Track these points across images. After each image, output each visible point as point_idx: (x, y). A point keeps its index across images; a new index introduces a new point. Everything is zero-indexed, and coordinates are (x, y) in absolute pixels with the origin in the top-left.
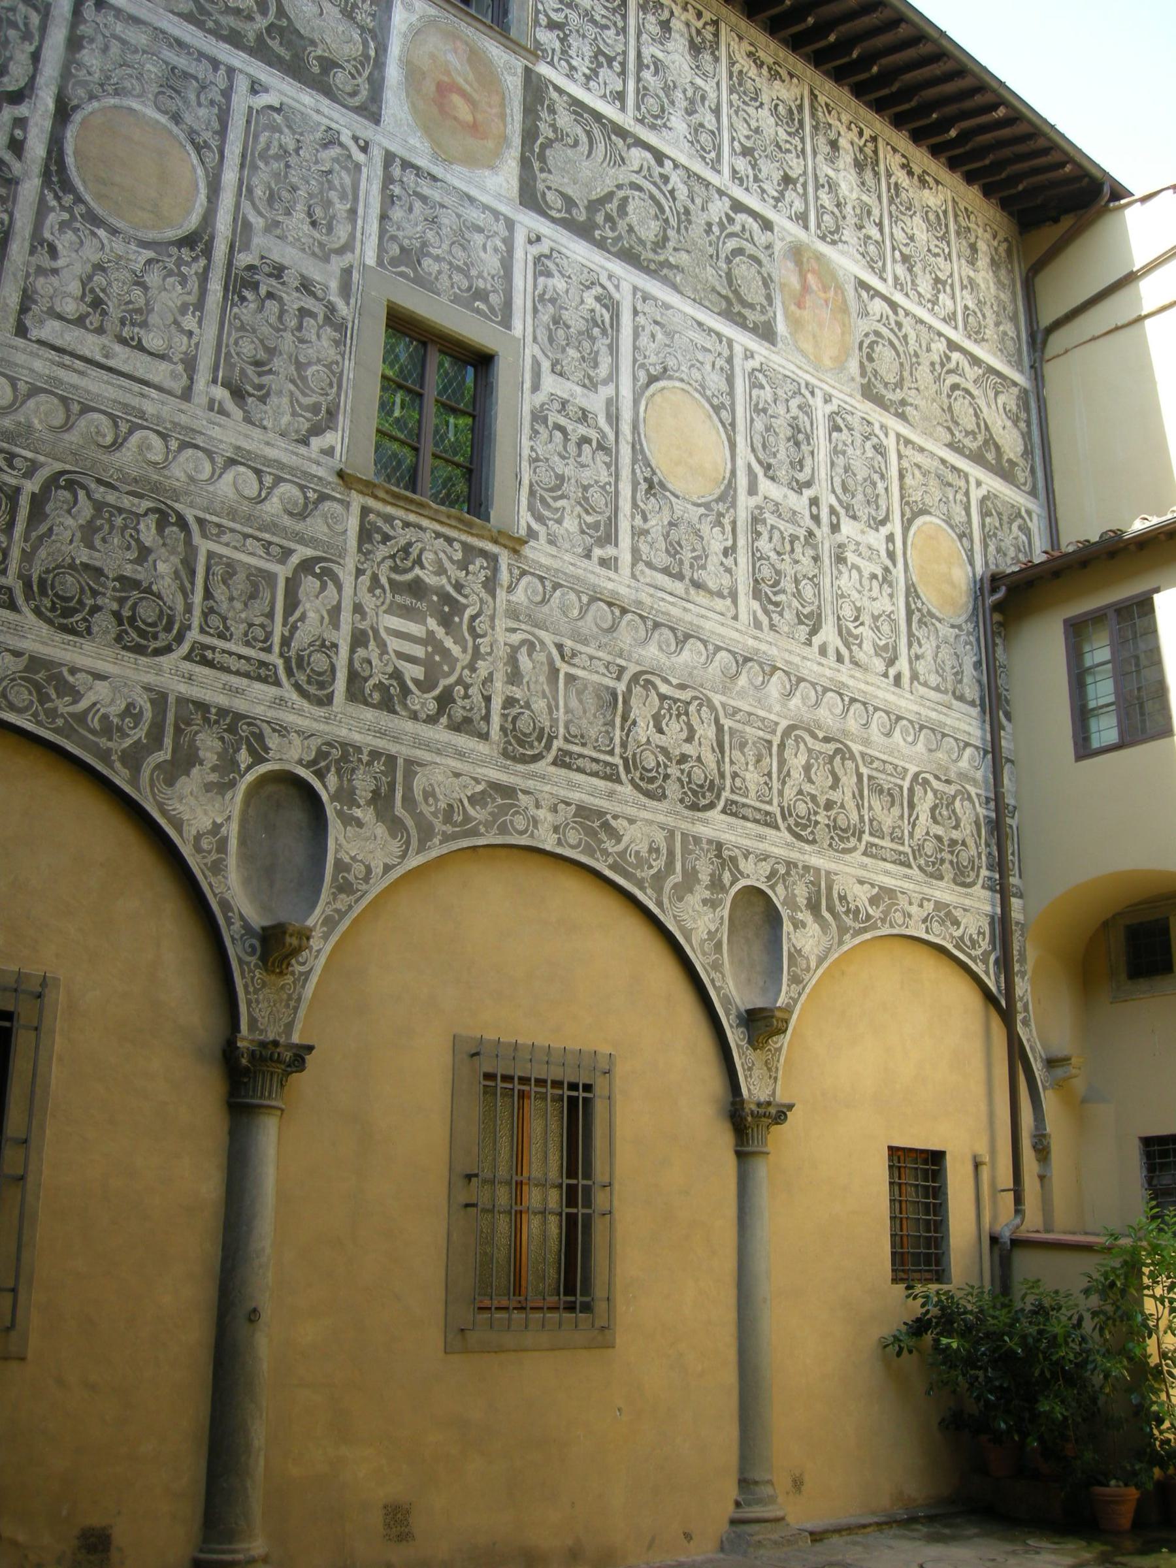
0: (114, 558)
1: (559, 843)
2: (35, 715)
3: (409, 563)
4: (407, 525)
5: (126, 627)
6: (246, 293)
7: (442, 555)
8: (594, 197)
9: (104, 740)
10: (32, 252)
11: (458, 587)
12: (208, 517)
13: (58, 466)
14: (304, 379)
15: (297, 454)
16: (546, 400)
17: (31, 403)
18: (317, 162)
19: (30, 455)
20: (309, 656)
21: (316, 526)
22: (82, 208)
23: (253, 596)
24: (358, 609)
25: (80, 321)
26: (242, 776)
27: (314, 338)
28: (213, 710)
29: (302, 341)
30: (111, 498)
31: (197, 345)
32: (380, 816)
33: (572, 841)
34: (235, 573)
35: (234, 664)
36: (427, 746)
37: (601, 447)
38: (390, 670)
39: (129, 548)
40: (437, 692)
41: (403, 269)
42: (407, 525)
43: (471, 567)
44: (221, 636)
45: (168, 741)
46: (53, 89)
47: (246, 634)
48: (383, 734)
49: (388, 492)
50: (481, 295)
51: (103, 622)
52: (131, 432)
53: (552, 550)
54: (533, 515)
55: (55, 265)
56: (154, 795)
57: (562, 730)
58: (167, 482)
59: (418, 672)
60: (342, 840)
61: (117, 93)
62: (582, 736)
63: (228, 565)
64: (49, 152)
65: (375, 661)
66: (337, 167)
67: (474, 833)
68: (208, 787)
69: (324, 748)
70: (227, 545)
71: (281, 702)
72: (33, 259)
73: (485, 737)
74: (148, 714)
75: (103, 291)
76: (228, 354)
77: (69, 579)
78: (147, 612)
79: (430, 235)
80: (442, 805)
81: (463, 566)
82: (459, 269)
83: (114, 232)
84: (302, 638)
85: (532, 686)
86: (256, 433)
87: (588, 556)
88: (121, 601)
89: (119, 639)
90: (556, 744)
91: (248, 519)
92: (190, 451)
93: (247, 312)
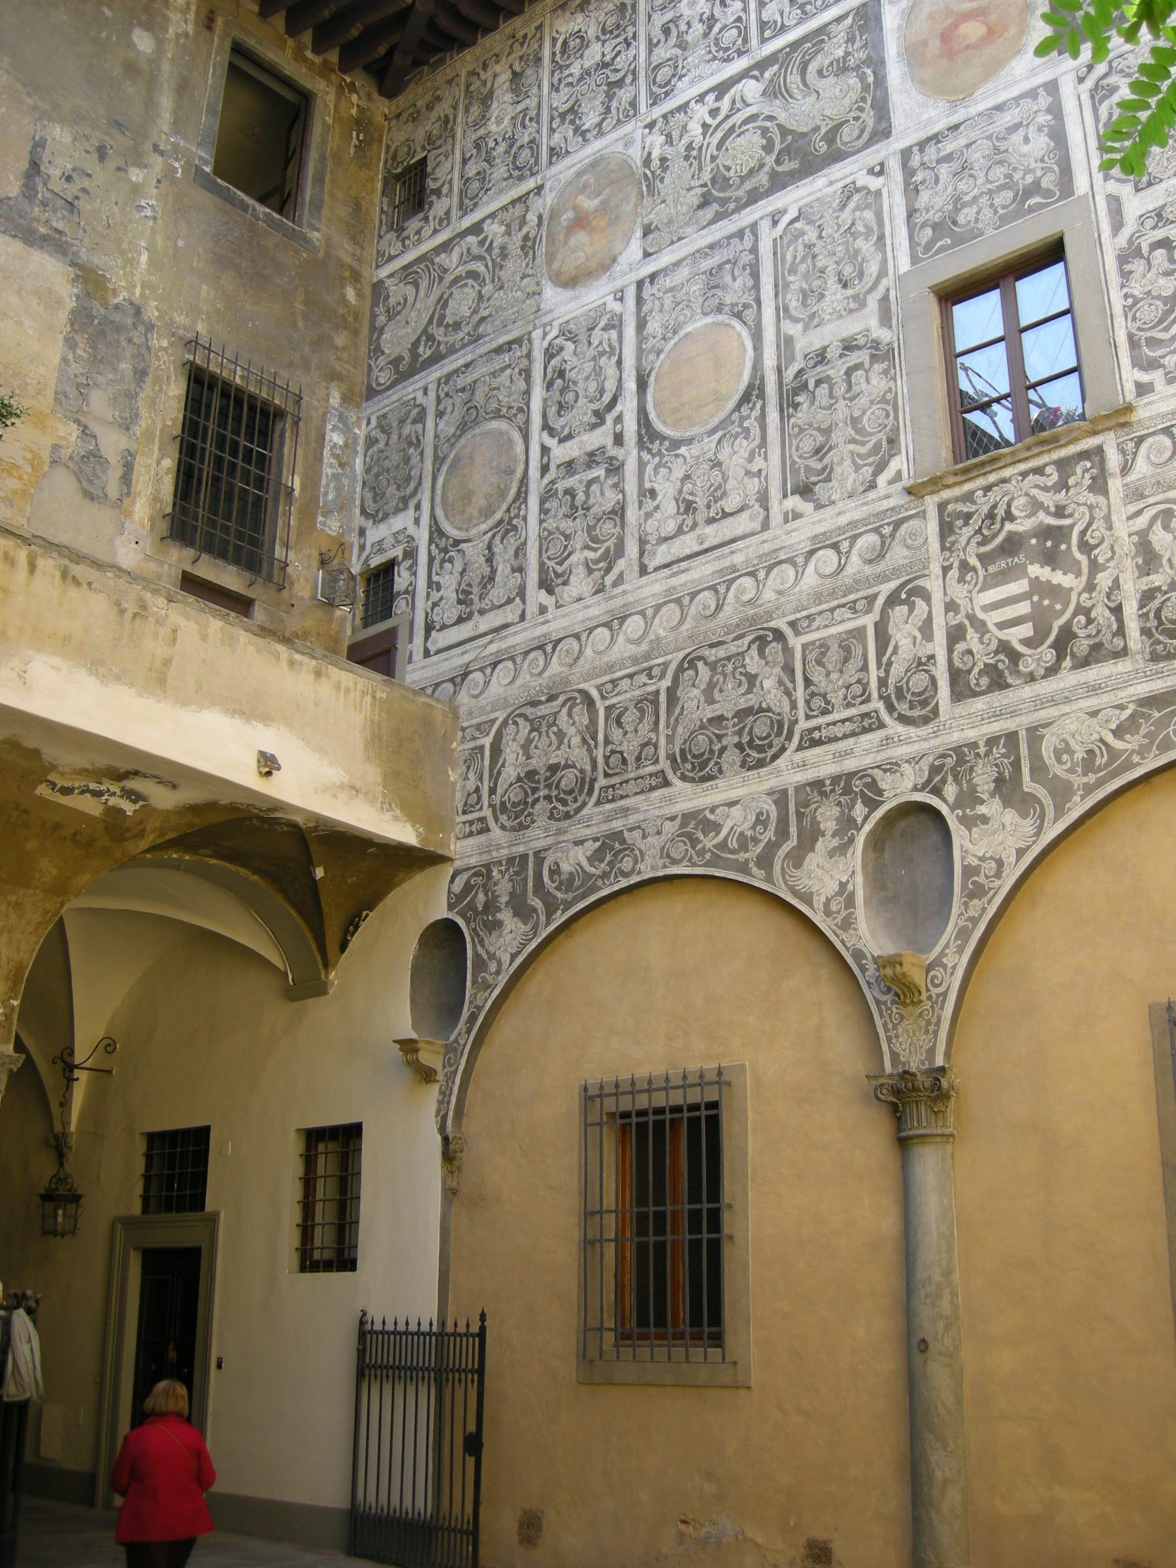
2: (690, 861)
3: (998, 526)
4: (987, 489)
5: (748, 751)
6: (799, 399)
7: (1035, 492)
10: (641, 503)
11: (1060, 512)
12: (798, 616)
13: (681, 655)
14: (859, 431)
15: (866, 504)
17: (657, 621)
18: (839, 226)
19: (660, 660)
21: (898, 555)
22: (667, 443)
23: (846, 660)
24: (951, 607)
25: (680, 531)
26: (859, 830)
27: (864, 385)
28: (828, 782)
30: (721, 653)
31: (766, 478)
32: (1007, 803)
34: (828, 649)
35: (839, 731)
36: (1053, 701)
38: (994, 645)
39: (740, 685)
42: (987, 489)
43: (1071, 481)
44: (825, 712)
45: (793, 830)
46: (634, 373)
47: (845, 698)
48: (998, 715)
49: (955, 474)
50: (1035, 188)
51: (732, 757)
52: (728, 589)
55: (656, 503)
58: (760, 610)
59: (1026, 630)
60: (967, 844)
61: (675, 332)
63: (821, 646)
65: (975, 646)
66: (858, 213)
67: (1128, 766)
68: (831, 854)
71: (888, 741)
73: (1124, 652)
74: (774, 815)
75: (692, 494)
77: (700, 737)
79: (962, 186)
80: (1080, 755)
81: (1063, 485)
82: (1000, 188)
84: (897, 670)
86: (828, 512)
88: (739, 733)
89: (743, 764)
91: (833, 594)
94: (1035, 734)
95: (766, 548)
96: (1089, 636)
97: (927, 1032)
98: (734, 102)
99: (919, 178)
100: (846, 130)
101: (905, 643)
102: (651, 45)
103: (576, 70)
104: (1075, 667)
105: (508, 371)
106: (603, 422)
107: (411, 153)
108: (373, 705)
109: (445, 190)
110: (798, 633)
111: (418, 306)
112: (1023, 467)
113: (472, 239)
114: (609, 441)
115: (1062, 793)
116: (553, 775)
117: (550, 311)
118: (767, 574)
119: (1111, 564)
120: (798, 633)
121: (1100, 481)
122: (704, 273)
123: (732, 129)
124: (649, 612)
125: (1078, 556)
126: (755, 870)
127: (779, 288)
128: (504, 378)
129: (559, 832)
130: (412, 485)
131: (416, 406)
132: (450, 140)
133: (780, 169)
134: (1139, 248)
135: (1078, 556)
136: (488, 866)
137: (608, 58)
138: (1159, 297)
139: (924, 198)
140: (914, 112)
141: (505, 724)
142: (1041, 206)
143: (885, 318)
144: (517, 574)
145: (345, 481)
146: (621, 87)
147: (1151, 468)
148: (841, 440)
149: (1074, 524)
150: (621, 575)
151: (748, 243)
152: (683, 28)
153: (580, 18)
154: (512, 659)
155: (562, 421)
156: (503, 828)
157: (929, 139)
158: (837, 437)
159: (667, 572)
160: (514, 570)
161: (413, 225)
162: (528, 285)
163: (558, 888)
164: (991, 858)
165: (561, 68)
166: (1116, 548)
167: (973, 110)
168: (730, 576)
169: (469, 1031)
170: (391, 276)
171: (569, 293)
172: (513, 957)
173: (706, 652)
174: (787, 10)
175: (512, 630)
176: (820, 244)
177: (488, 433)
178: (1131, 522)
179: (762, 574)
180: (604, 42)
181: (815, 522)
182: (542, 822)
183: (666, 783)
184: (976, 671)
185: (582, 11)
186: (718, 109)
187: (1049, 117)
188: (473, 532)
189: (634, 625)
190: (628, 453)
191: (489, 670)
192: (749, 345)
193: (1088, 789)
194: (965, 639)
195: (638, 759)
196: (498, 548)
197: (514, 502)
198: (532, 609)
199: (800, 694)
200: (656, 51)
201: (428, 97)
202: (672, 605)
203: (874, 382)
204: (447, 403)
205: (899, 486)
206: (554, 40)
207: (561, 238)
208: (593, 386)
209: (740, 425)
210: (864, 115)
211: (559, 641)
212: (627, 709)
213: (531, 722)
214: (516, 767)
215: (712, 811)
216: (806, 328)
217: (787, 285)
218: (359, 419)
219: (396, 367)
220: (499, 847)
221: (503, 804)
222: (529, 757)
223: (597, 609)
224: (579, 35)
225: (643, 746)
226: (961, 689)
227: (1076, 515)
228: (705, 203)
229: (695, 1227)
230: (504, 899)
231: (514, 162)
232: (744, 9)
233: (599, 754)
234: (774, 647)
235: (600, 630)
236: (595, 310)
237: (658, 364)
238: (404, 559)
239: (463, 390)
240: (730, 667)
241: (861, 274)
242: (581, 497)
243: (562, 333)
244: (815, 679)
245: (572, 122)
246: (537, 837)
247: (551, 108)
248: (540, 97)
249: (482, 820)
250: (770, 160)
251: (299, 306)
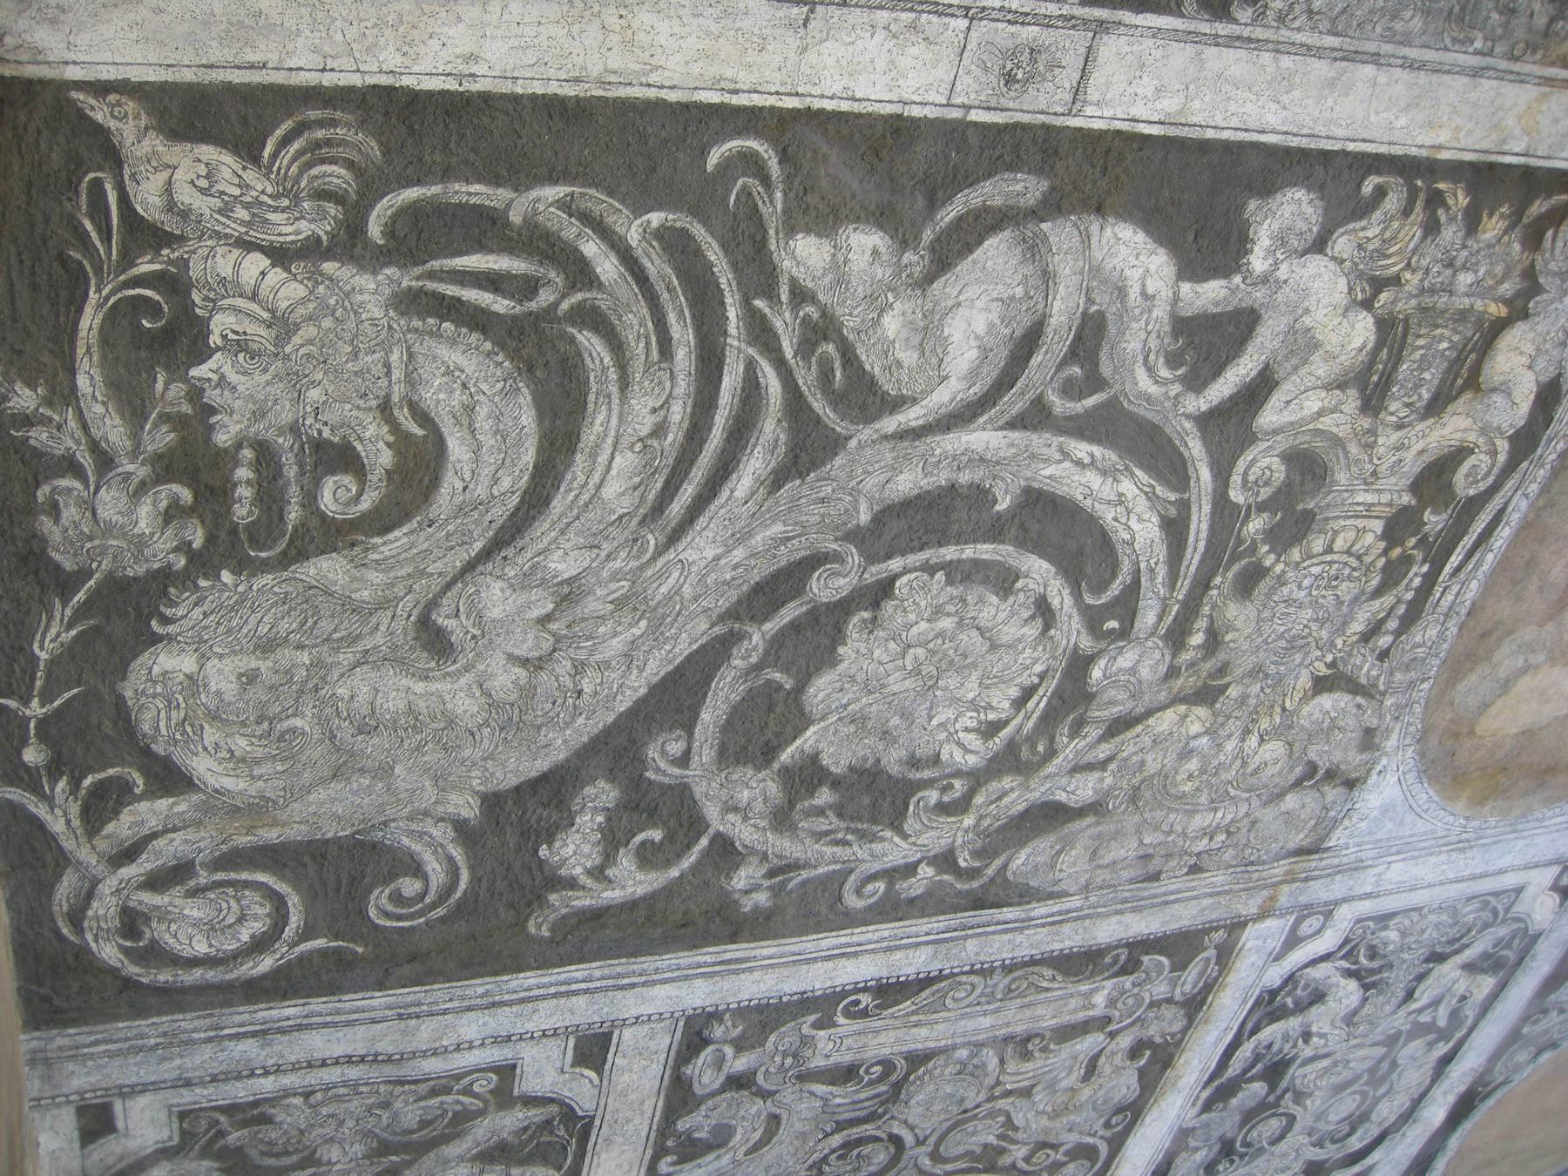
113: (1133, 257)
162: (1327, 730)
171: (1437, 816)
236: (1482, 901)
239: (846, 1074)
243: (1348, 948)
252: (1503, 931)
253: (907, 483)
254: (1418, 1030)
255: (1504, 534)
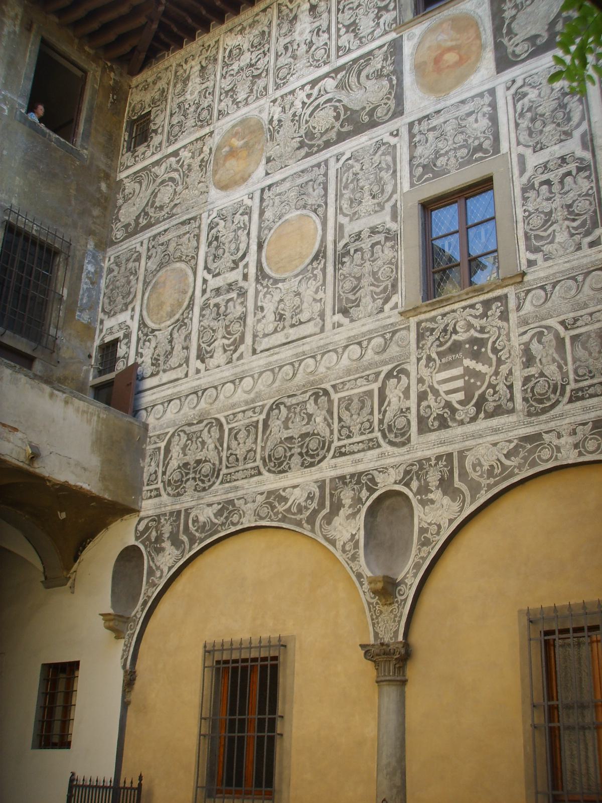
0: (297, 428)
1: (580, 454)
6: (345, 260)
7: (469, 318)
8: (552, 17)
9: (299, 516)
10: (255, 314)
12: (338, 382)
13: (272, 401)
15: (378, 320)
16: (532, 173)
17: (260, 381)
18: (373, 164)
19: (260, 403)
20: (394, 423)
21: (394, 350)
22: (271, 281)
23: (362, 408)
24: (421, 381)
25: (276, 331)
26: (363, 505)
27: (380, 253)
28: (348, 477)
29: (373, 261)
30: (294, 401)
32: (445, 493)
33: (591, 449)
34: (352, 401)
36: (474, 437)
37: (579, 169)
38: (442, 404)
39: (303, 419)
40: (474, 401)
41: (426, 177)
42: (444, 315)
43: (489, 313)
44: (349, 437)
45: (328, 503)
47: (360, 429)
48: (442, 443)
49: (427, 306)
50: (479, 148)
51: (296, 460)
52: (300, 365)
53: (550, 263)
54: (531, 252)
55: (263, 314)
56: (321, 532)
57: (572, 376)
58: (317, 378)
59: (461, 396)
60: (422, 515)
61: (280, 219)
62: (590, 372)
63: (348, 400)
64: (257, 267)
65: (432, 403)
66: (383, 157)
68: (348, 518)
69: (408, 469)
70: (348, 390)
72: (256, 319)
73: (512, 411)
74: (317, 494)
75: (283, 310)
76: (340, 295)
77: (280, 448)
78: (313, 445)
79: (440, 145)
80: (486, 467)
83: (284, 280)
85: (544, 360)
86: (358, 323)
87: (579, 248)
88: (301, 447)
90: (568, 389)
91: (357, 370)
92: (326, 355)
93: (345, 270)
94: (462, 454)
95: (322, 343)
96: (495, 401)
97: (394, 621)
98: (320, 91)
99: (416, 139)
100: (379, 110)
101: (394, 400)
102: (277, 56)
103: (235, 67)
104: (485, 418)
105: (188, 235)
106: (237, 267)
107: (143, 108)
108: (98, 421)
109: (159, 131)
110: (336, 392)
111: (141, 195)
112: (464, 304)
113: (173, 160)
114: (240, 278)
115: (475, 488)
116: (198, 465)
117: (212, 203)
118: (322, 357)
119: (508, 361)
120: (336, 392)
121: (505, 314)
122: (298, 186)
123: (318, 106)
124: (256, 376)
125: (491, 355)
126: (305, 525)
127: (338, 196)
128: (185, 239)
129: (199, 498)
130: (131, 296)
131: (136, 252)
132: (164, 102)
133: (343, 130)
134: (533, 184)
135: (491, 355)
136: (158, 516)
137: (253, 62)
138: (542, 212)
139: (419, 150)
140: (416, 101)
141: (173, 435)
142: (482, 158)
143: (394, 217)
144: (185, 350)
145: (94, 293)
146: (259, 79)
147: (533, 308)
148: (366, 284)
149: (490, 337)
150: (242, 354)
151: (322, 171)
152: (295, 47)
153: (240, 37)
154: (179, 398)
155: (215, 265)
156: (169, 494)
157: (424, 117)
158: (365, 282)
159: (267, 353)
160: (183, 348)
161: (141, 149)
163: (197, 531)
164: (435, 524)
165: (228, 65)
166: (512, 352)
167: (449, 103)
168: (300, 358)
169: (142, 610)
170: (127, 177)
171: (223, 193)
172: (170, 568)
173: (286, 400)
174: (352, 41)
175: (180, 382)
176: (361, 173)
177: (174, 269)
178: (521, 337)
179: (319, 357)
180: (252, 52)
181: (350, 329)
182: (190, 492)
183: (260, 473)
184: (432, 417)
185: (241, 33)
186: (311, 94)
187: (490, 109)
188: (163, 325)
189: (247, 382)
190: (250, 285)
191: (166, 404)
192: (320, 227)
193: (490, 487)
194: (427, 399)
195: (245, 459)
196: (175, 335)
197: (186, 309)
198: (192, 371)
199: (336, 426)
200: (280, 59)
201: (154, 77)
202: (268, 373)
203: (386, 252)
204: (153, 251)
205: (396, 311)
206: (225, 49)
207: (221, 162)
208: (233, 246)
209: (312, 273)
210: (389, 102)
211: (206, 389)
212: (240, 430)
213: (188, 435)
214: (178, 460)
215: (284, 490)
216: (351, 220)
217: (342, 195)
218: (104, 258)
219: (127, 230)
220: (166, 506)
221: (169, 481)
222: (185, 455)
223: (228, 372)
224: (239, 47)
225: (248, 452)
226: (424, 427)
227: (491, 332)
228: (302, 145)
229: (261, 728)
230: (167, 535)
231: (198, 117)
232: (329, 39)
233: (224, 455)
234: (323, 399)
235: (228, 384)
237: (269, 236)
238: (123, 339)
239: (162, 244)
240: (298, 409)
241: (383, 191)
242: (222, 309)
244: (344, 418)
245: (232, 96)
246: (187, 501)
247: (221, 88)
248: (215, 81)
249: (157, 489)
250: (337, 125)
251: (73, 192)
252: (244, 207)
253: (160, 181)
254: (240, 228)
255: (212, 162)
